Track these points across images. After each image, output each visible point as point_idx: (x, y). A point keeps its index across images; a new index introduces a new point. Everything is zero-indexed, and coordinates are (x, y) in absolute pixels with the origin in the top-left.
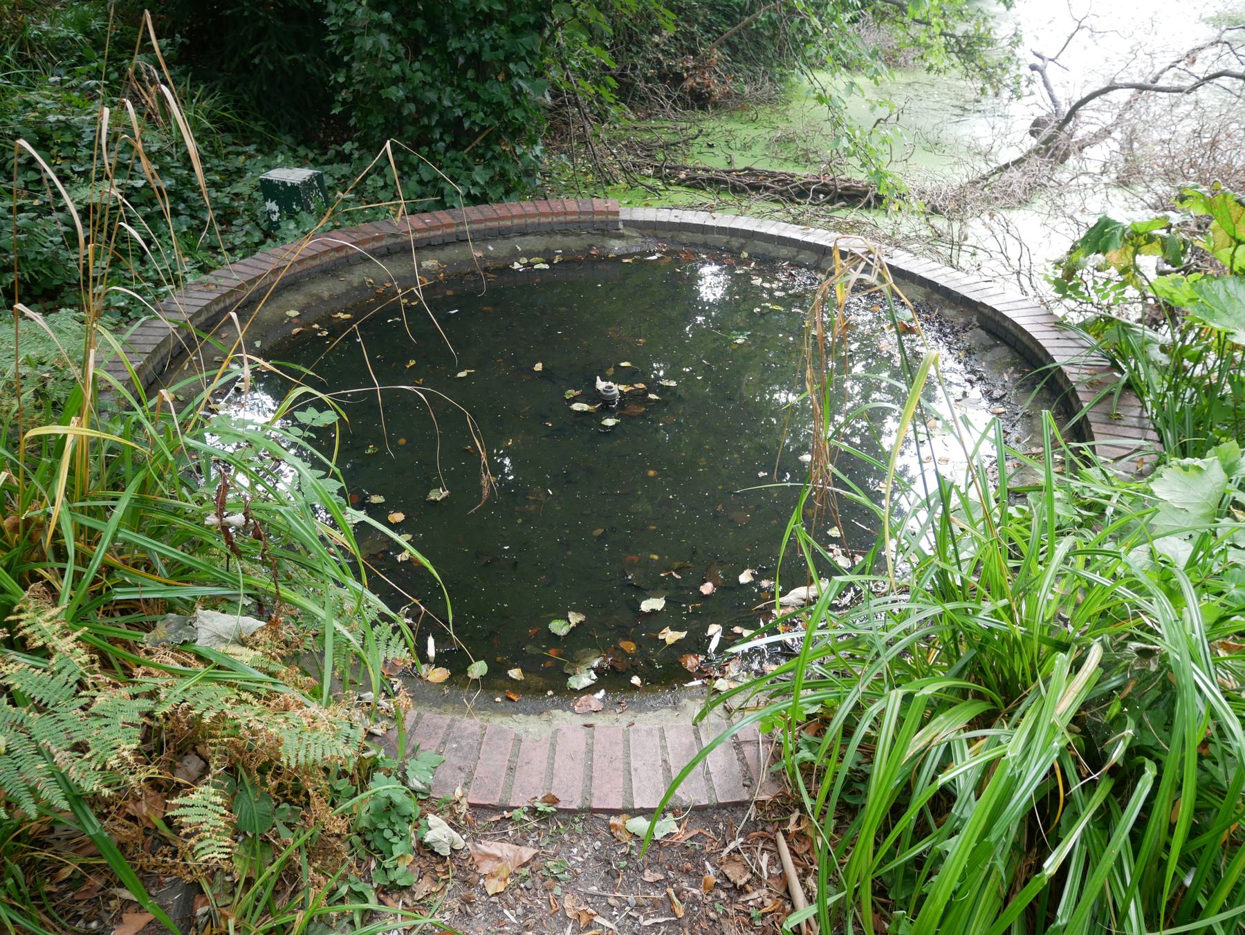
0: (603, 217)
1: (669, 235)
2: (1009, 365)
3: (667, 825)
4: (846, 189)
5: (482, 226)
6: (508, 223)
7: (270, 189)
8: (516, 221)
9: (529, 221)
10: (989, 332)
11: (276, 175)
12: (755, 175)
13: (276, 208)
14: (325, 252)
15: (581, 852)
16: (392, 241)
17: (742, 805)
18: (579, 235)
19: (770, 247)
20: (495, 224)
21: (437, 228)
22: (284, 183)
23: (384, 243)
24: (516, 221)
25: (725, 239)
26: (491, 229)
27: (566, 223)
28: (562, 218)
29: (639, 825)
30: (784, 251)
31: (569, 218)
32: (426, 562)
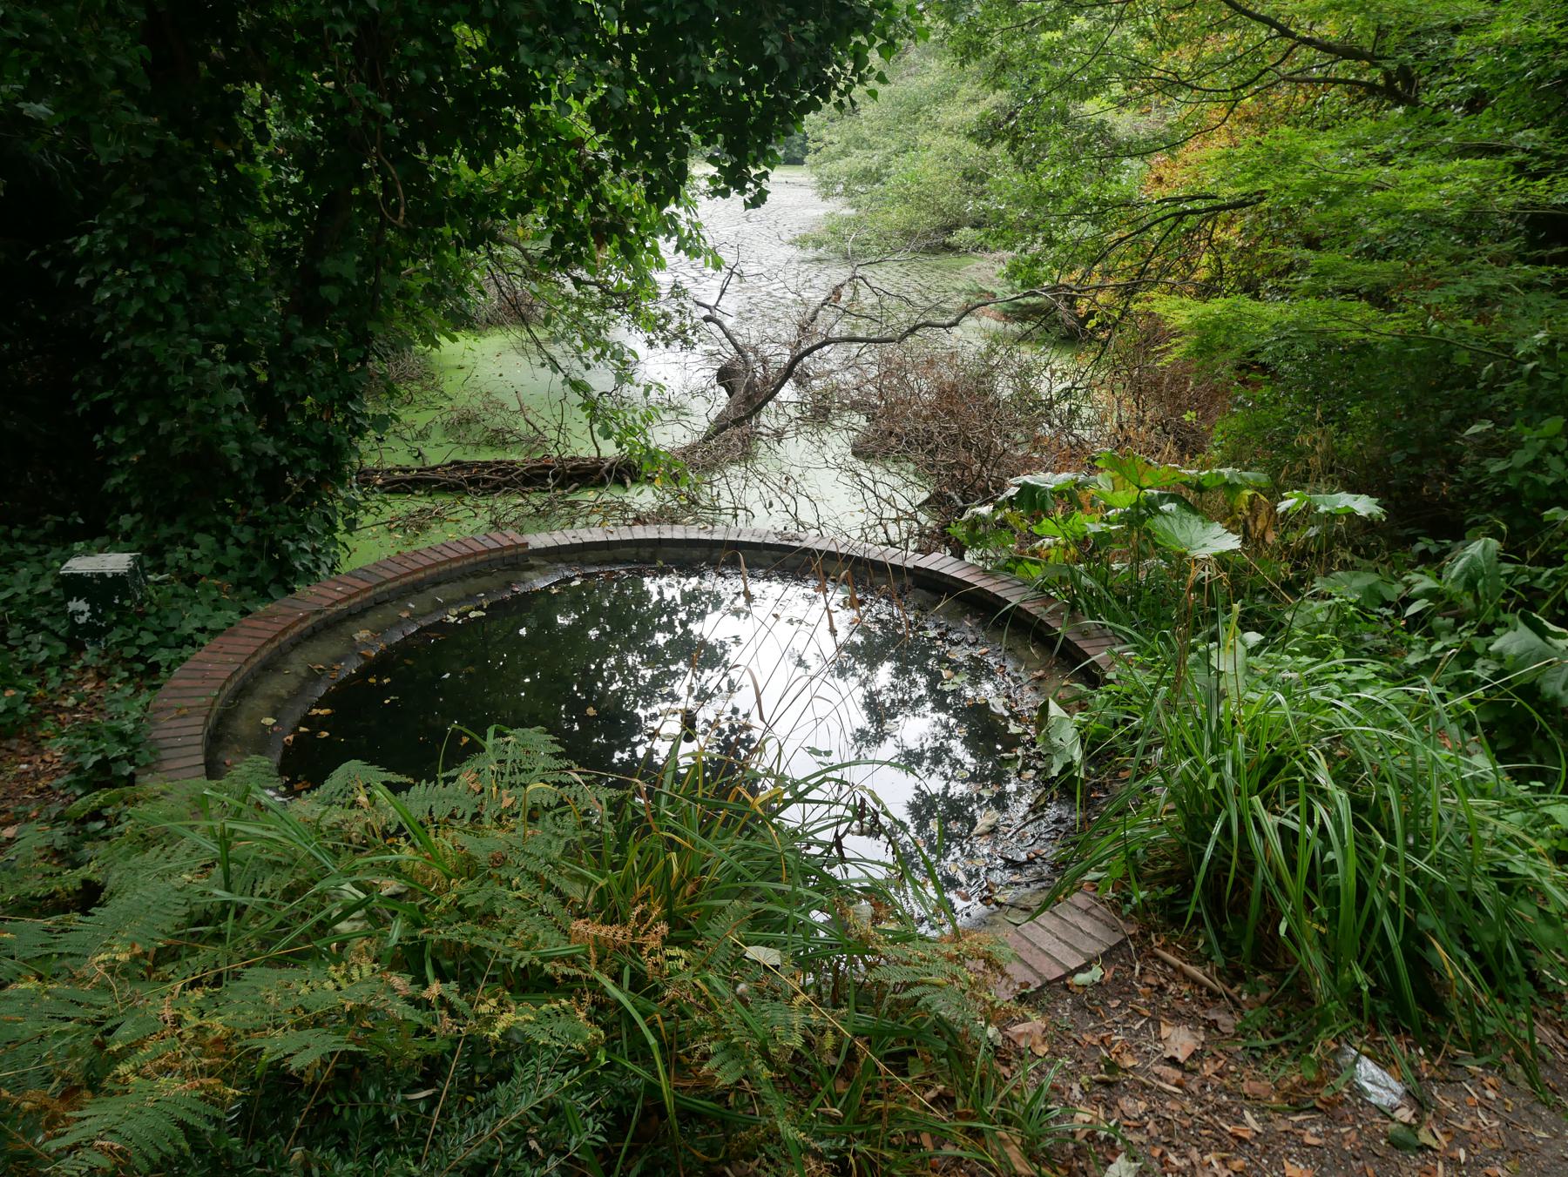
0: (513, 551)
1: (575, 556)
2: (963, 614)
3: (1096, 973)
4: (573, 468)
5: (397, 583)
6: (422, 575)
7: (77, 585)
8: (429, 572)
9: (441, 568)
10: (928, 589)
11: (81, 565)
12: (465, 468)
13: (86, 607)
14: (264, 645)
15: (1065, 1009)
16: (316, 618)
17: (1122, 943)
18: (491, 574)
19: (681, 551)
20: (410, 578)
21: (356, 595)
22: (102, 576)
23: (309, 622)
24: (429, 572)
25: (633, 551)
26: (406, 585)
27: (476, 564)
28: (472, 560)
29: (1081, 978)
30: (696, 553)
31: (479, 558)
32: (1546, 623)
